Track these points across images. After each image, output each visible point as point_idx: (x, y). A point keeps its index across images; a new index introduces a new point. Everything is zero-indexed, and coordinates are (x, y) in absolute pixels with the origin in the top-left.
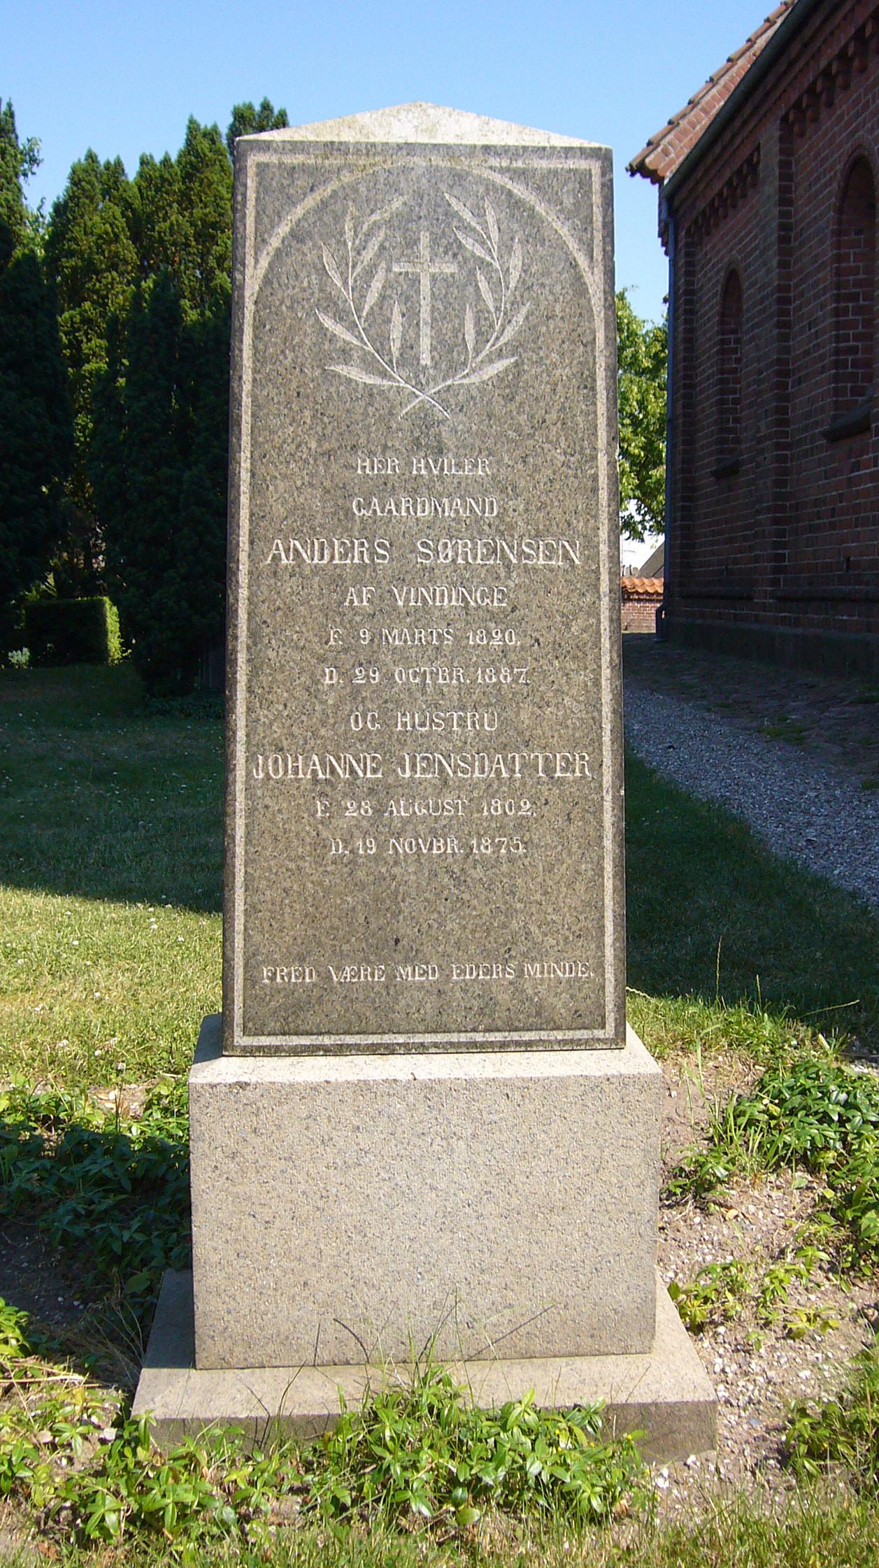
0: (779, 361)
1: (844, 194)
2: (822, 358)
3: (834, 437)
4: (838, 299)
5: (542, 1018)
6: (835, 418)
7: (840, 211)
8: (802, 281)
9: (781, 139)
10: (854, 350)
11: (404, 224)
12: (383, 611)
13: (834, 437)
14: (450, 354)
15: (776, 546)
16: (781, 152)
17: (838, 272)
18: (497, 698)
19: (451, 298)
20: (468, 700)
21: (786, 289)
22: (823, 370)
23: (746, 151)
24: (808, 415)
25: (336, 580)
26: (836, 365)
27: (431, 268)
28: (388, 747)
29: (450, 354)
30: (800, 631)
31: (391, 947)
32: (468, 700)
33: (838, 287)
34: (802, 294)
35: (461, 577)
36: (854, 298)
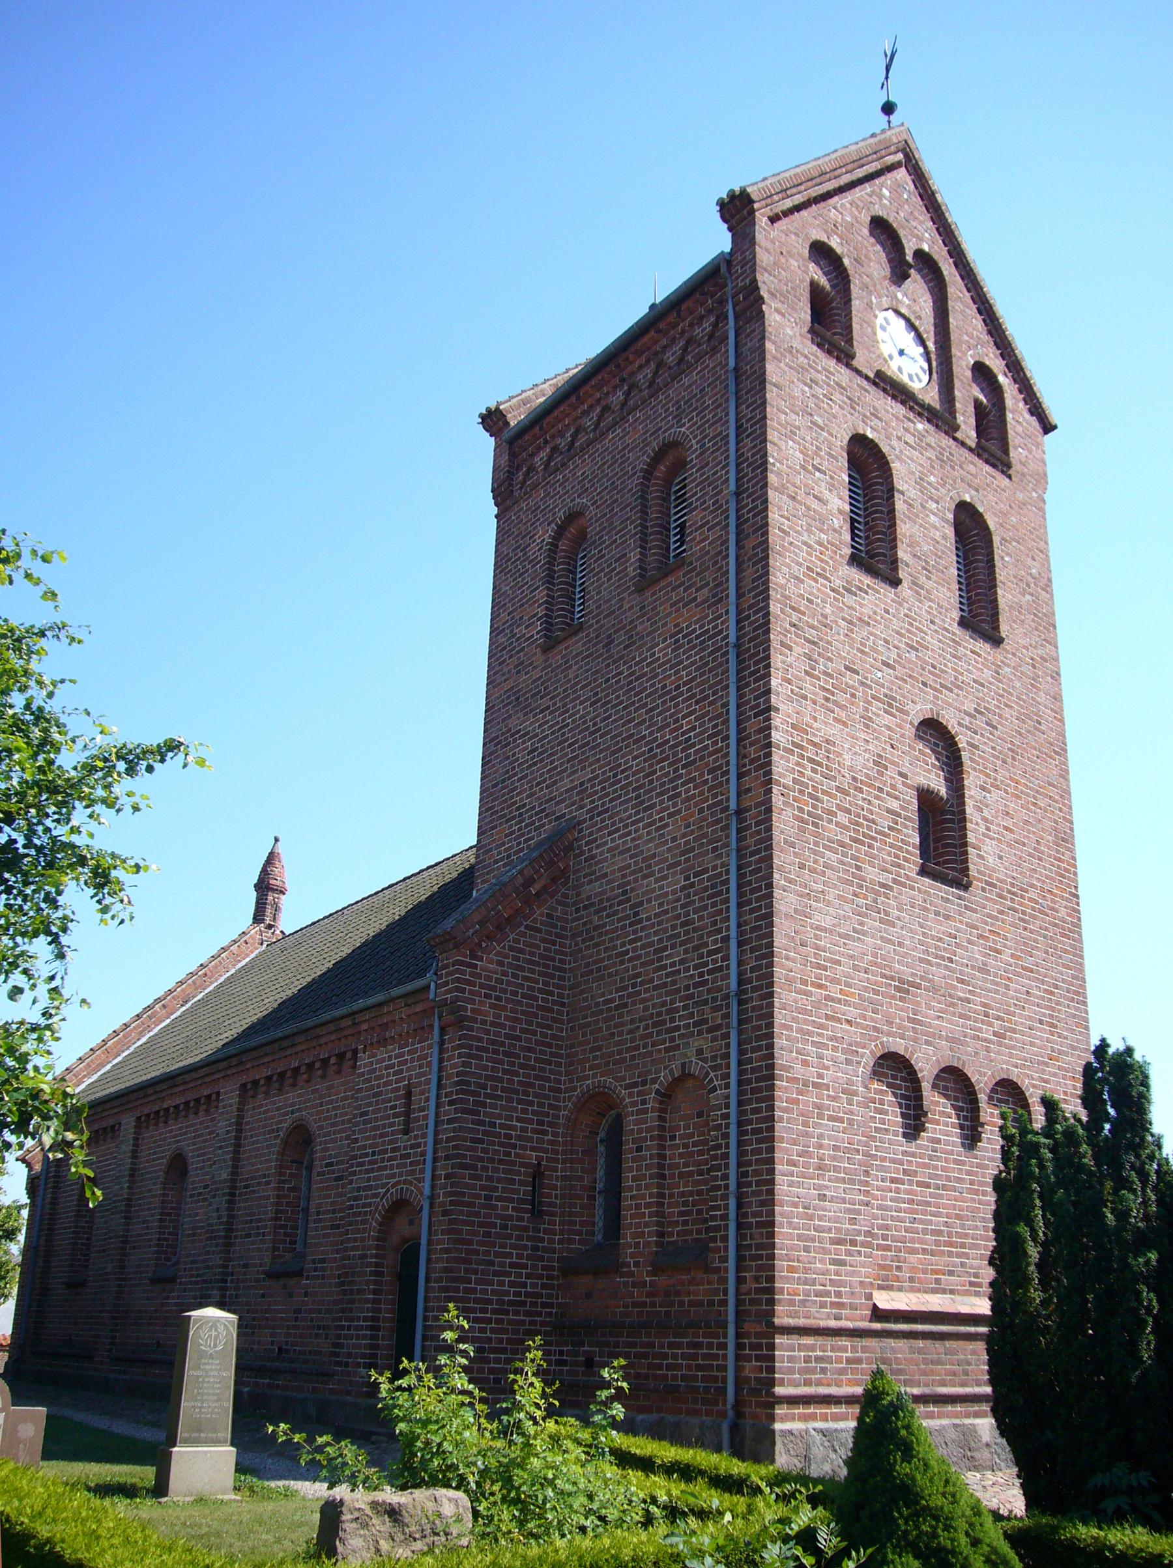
0: (123, 1236)
1: (170, 1166)
2: (150, 1240)
3: (155, 1281)
4: (162, 1214)
5: (220, 1442)
6: (155, 1271)
7: (167, 1173)
8: (140, 1199)
9: (136, 1127)
10: (167, 1240)
11: (211, 1327)
12: (203, 1381)
13: (155, 1281)
14: (215, 1346)
15: (112, 1331)
16: (135, 1133)
17: (163, 1202)
18: (217, 1394)
19: (216, 1337)
20: (214, 1394)
21: (130, 1200)
22: (150, 1246)
23: (112, 1121)
24: (138, 1266)
25: (198, 1377)
26: (158, 1245)
27: (214, 1333)
28: (202, 1401)
29: (215, 1346)
30: (126, 1377)
31: (200, 1431)
32: (214, 1394)
33: (163, 1208)
34: (140, 1205)
35: (214, 1377)
36: (169, 1214)
